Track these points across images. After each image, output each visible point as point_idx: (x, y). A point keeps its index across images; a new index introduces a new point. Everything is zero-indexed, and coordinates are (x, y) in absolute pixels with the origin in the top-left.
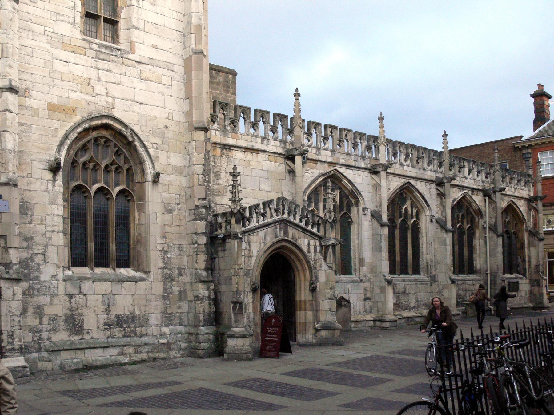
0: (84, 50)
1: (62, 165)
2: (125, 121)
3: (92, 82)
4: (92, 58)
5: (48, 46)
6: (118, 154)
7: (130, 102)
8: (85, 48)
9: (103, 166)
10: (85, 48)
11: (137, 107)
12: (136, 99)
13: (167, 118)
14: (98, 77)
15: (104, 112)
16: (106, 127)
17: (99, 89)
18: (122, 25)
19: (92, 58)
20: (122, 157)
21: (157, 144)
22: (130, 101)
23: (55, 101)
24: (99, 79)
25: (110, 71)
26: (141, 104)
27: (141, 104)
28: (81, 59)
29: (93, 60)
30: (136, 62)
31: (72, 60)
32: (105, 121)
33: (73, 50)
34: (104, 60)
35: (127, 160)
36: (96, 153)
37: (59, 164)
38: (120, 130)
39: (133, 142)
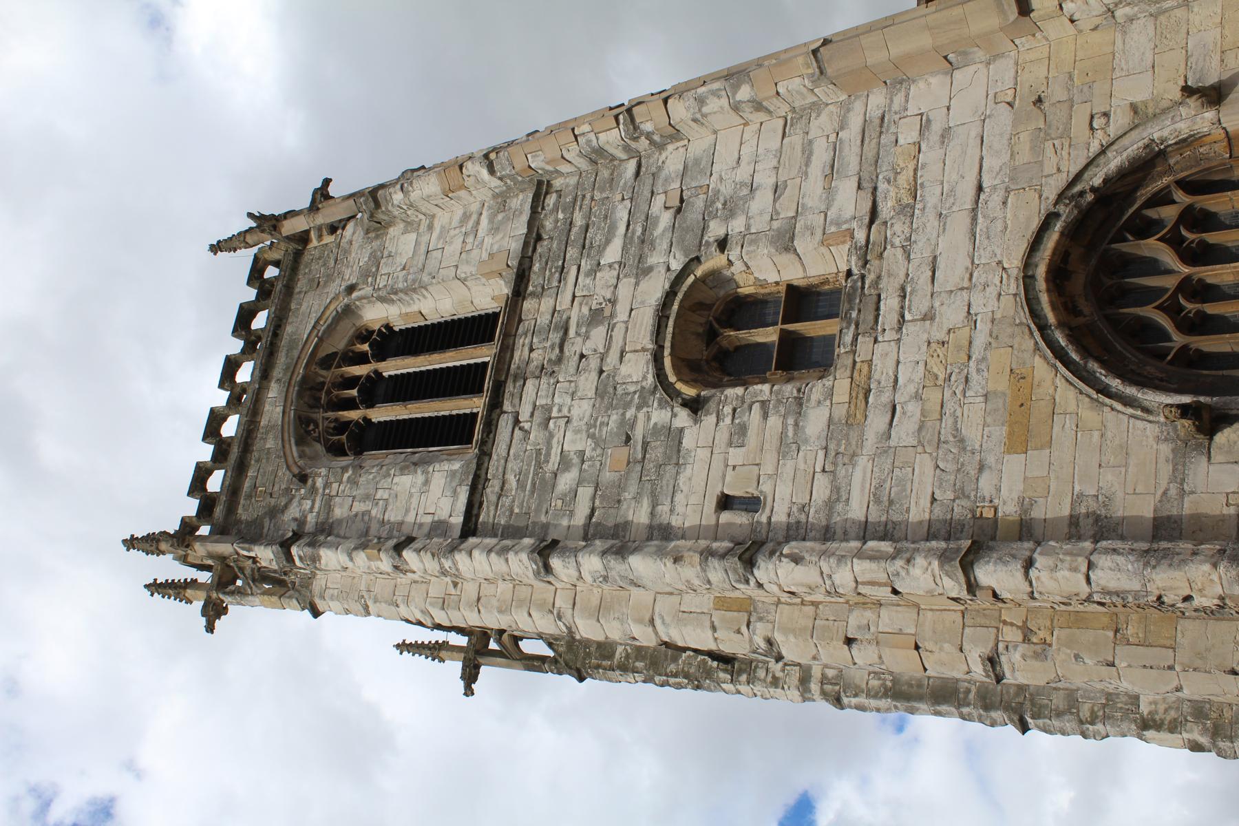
0: (858, 366)
1: (1186, 399)
2: (1035, 224)
3: (941, 336)
4: (876, 341)
5: (863, 461)
6: (1145, 228)
7: (980, 220)
8: (855, 362)
9: (1186, 270)
10: (855, 362)
11: (993, 200)
12: (969, 206)
13: (1010, 104)
14: (923, 319)
15: (1013, 286)
16: (1058, 275)
17: (951, 314)
18: (793, 274)
19: (876, 341)
20: (1152, 213)
21: (1092, 117)
22: (974, 220)
23: (999, 432)
24: (929, 316)
25: (903, 289)
26: (980, 189)
27: (980, 189)
28: (882, 370)
29: (880, 339)
30: (872, 222)
31: (886, 398)
32: (1041, 284)
33: (861, 396)
34: (878, 309)
35: (1163, 198)
36: (1149, 295)
37: (1184, 410)
38: (1062, 234)
39: (1093, 189)
